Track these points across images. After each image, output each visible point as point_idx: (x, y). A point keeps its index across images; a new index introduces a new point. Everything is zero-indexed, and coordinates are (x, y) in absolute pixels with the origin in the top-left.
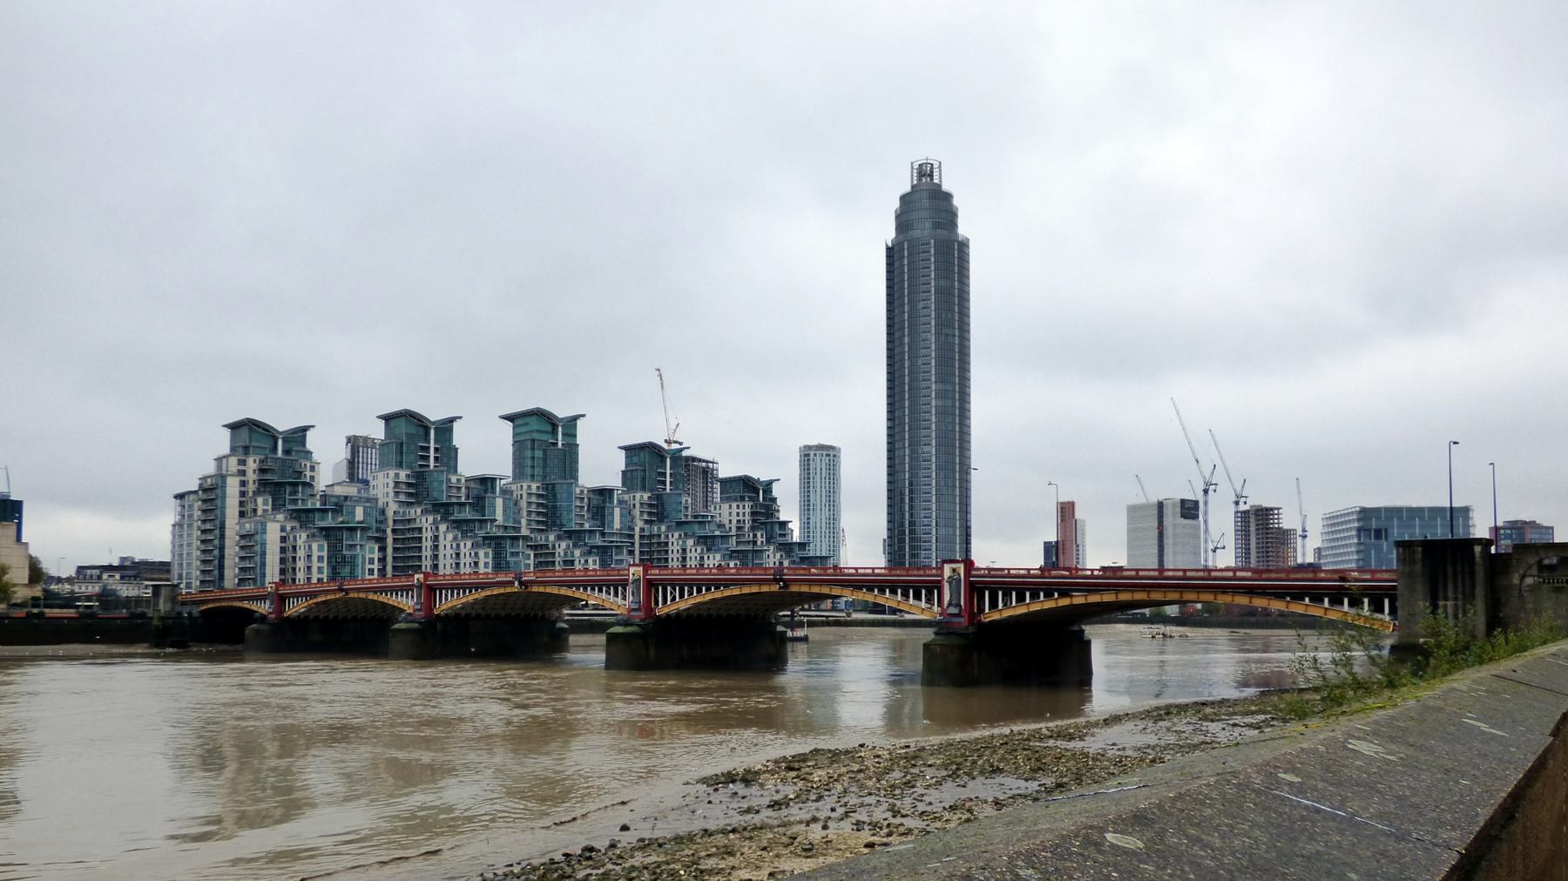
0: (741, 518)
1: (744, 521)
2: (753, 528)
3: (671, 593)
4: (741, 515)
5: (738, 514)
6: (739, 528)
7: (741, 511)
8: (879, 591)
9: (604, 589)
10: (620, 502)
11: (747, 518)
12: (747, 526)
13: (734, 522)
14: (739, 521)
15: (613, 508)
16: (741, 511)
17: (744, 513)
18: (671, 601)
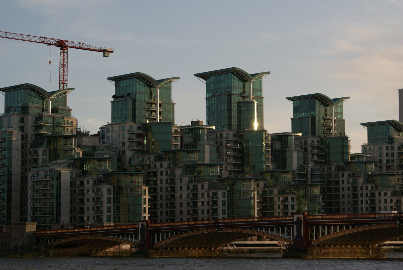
0: (390, 158)
1: (393, 161)
4: (390, 155)
6: (388, 167)
7: (390, 152)
8: (260, 229)
11: (396, 157)
13: (385, 161)
17: (393, 155)
18: (162, 240)
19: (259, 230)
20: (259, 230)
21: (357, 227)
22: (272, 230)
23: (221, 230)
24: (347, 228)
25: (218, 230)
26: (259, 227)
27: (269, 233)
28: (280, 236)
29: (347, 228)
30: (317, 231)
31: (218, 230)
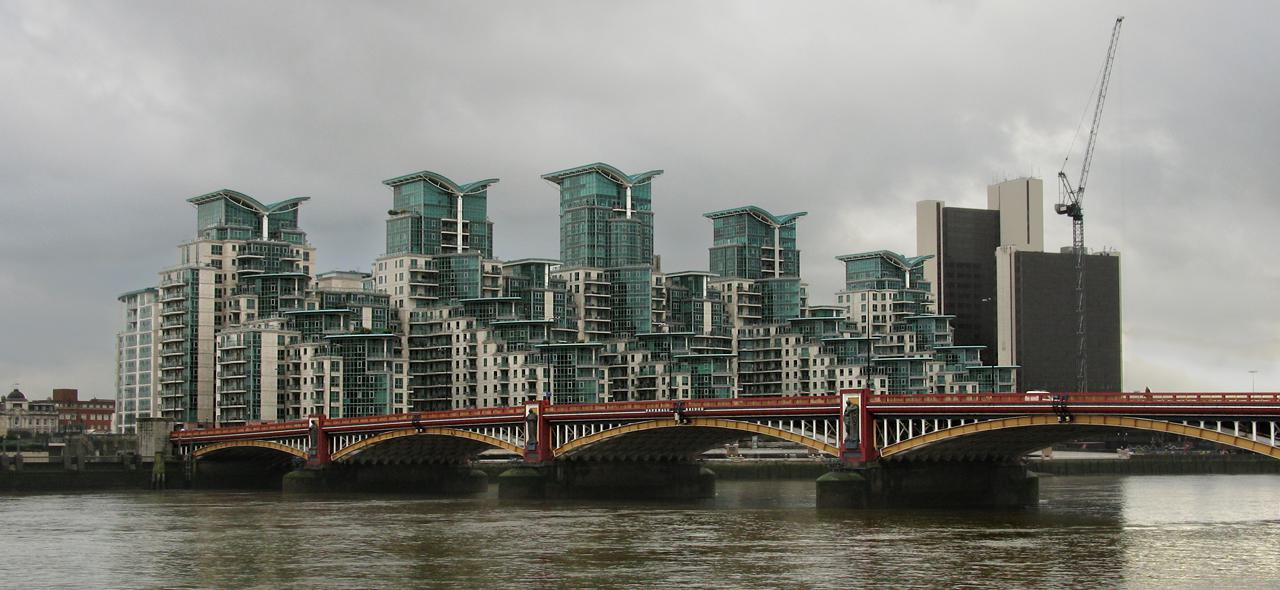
0: (879, 313)
1: (884, 317)
2: (897, 328)
3: (569, 432)
4: (879, 308)
5: (875, 307)
6: (877, 328)
7: (879, 303)
9: (501, 429)
10: (554, 283)
11: (889, 312)
12: (889, 324)
14: (876, 318)
15: (543, 293)
16: (879, 303)
17: (884, 306)
19: (770, 425)
20: (770, 425)
21: (976, 421)
22: (798, 425)
23: (1072, 418)
24: (956, 423)
25: (1063, 419)
26: (770, 418)
27: (791, 431)
28: (814, 438)
29: (956, 423)
30: (892, 425)
31: (1063, 419)
